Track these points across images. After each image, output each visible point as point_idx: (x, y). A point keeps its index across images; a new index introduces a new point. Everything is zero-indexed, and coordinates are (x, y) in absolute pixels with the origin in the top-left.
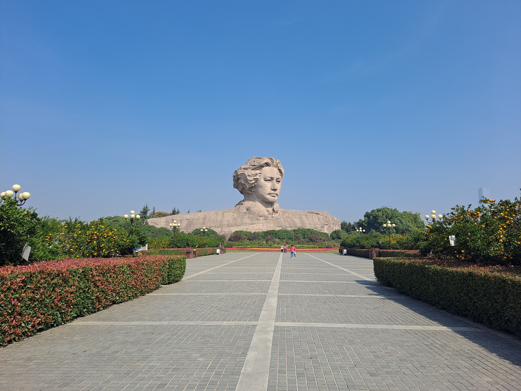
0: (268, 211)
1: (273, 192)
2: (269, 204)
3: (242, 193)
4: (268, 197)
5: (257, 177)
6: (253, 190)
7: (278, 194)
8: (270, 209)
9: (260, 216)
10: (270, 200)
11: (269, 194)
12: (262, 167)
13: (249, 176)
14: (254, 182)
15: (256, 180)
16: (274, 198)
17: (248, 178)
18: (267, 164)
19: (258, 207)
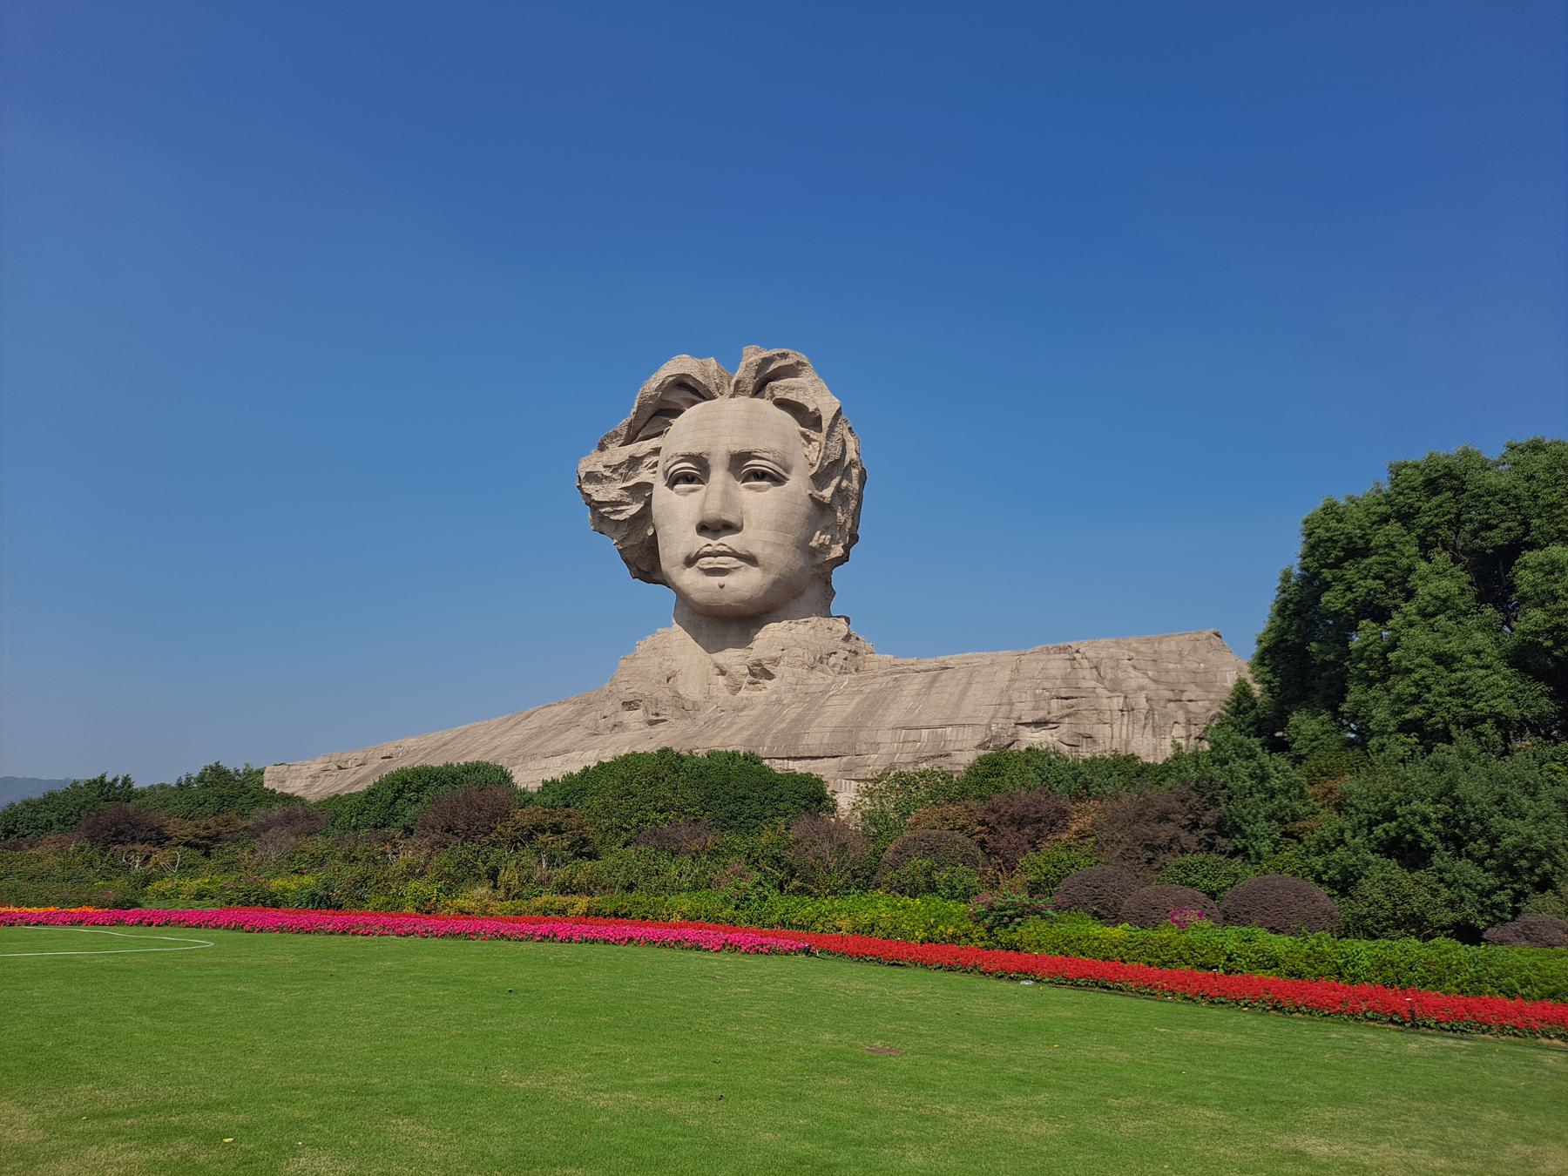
0: (723, 673)
1: (703, 541)
2: (727, 623)
4: (690, 580)
5: (644, 475)
7: (756, 550)
8: (732, 657)
9: (629, 705)
10: (697, 596)
11: (690, 561)
12: (660, 413)
13: (592, 477)
14: (635, 508)
15: (642, 491)
16: (716, 580)
17: (600, 493)
18: (690, 390)
19: (680, 648)
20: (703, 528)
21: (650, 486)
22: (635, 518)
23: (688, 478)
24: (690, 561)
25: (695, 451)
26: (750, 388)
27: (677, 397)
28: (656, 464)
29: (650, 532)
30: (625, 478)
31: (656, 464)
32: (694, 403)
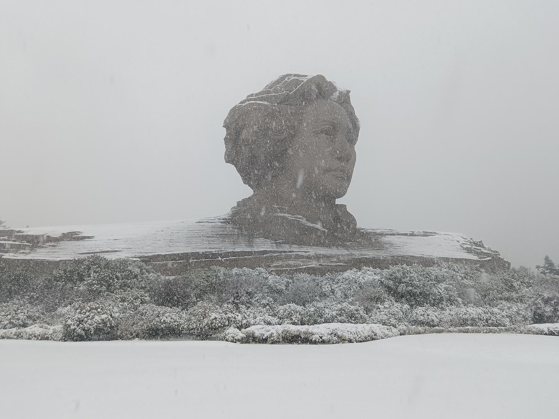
3: (247, 180)
20: (339, 159)
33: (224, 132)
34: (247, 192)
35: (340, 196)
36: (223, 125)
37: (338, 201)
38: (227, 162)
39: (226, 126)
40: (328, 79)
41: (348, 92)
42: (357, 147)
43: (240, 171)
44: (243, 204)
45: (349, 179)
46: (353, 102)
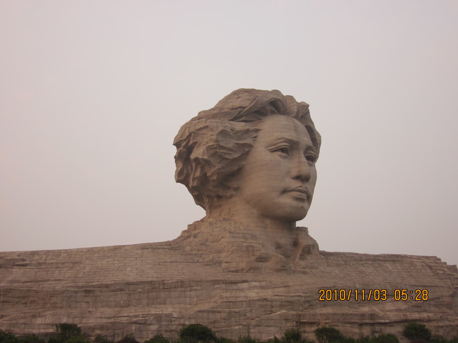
1: (296, 184)
3: (199, 200)
5: (248, 141)
6: (234, 184)
11: (285, 191)
14: (236, 155)
20: (298, 178)
21: (250, 146)
22: (235, 160)
23: (283, 150)
24: (285, 191)
25: (295, 139)
26: (300, 116)
27: (269, 108)
28: (256, 137)
29: (236, 168)
30: (239, 139)
31: (256, 137)
32: (273, 113)
33: (174, 151)
34: (199, 213)
35: (301, 218)
36: (172, 142)
37: (299, 224)
38: (177, 181)
39: (177, 144)
40: (285, 93)
41: (308, 106)
42: (318, 164)
43: (192, 190)
44: (194, 227)
45: (309, 198)
46: (314, 116)
